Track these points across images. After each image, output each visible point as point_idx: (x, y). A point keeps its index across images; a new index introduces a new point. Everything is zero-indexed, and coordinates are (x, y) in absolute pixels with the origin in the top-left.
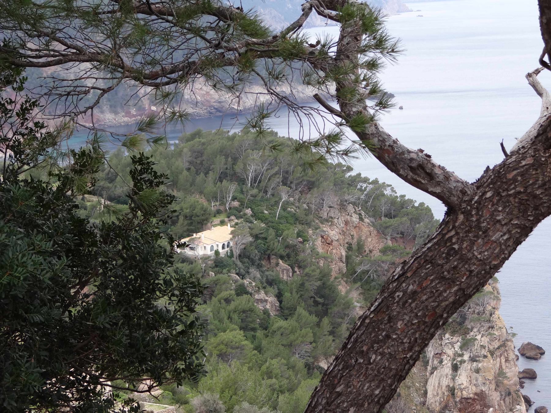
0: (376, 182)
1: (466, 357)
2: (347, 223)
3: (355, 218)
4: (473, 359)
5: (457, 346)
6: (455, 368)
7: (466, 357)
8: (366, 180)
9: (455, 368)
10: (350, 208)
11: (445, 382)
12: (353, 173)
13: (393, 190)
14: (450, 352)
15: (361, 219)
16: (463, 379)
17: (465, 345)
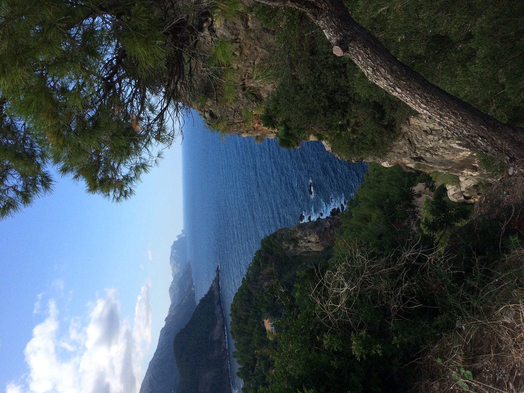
0: (248, 269)
1: (306, 238)
2: (262, 279)
3: (261, 276)
4: (306, 236)
5: (302, 241)
6: (309, 242)
7: (306, 238)
8: (247, 273)
9: (309, 242)
10: (257, 278)
11: (314, 245)
12: (245, 277)
13: (251, 264)
14: (304, 243)
15: (261, 274)
16: (313, 239)
17: (302, 239)
